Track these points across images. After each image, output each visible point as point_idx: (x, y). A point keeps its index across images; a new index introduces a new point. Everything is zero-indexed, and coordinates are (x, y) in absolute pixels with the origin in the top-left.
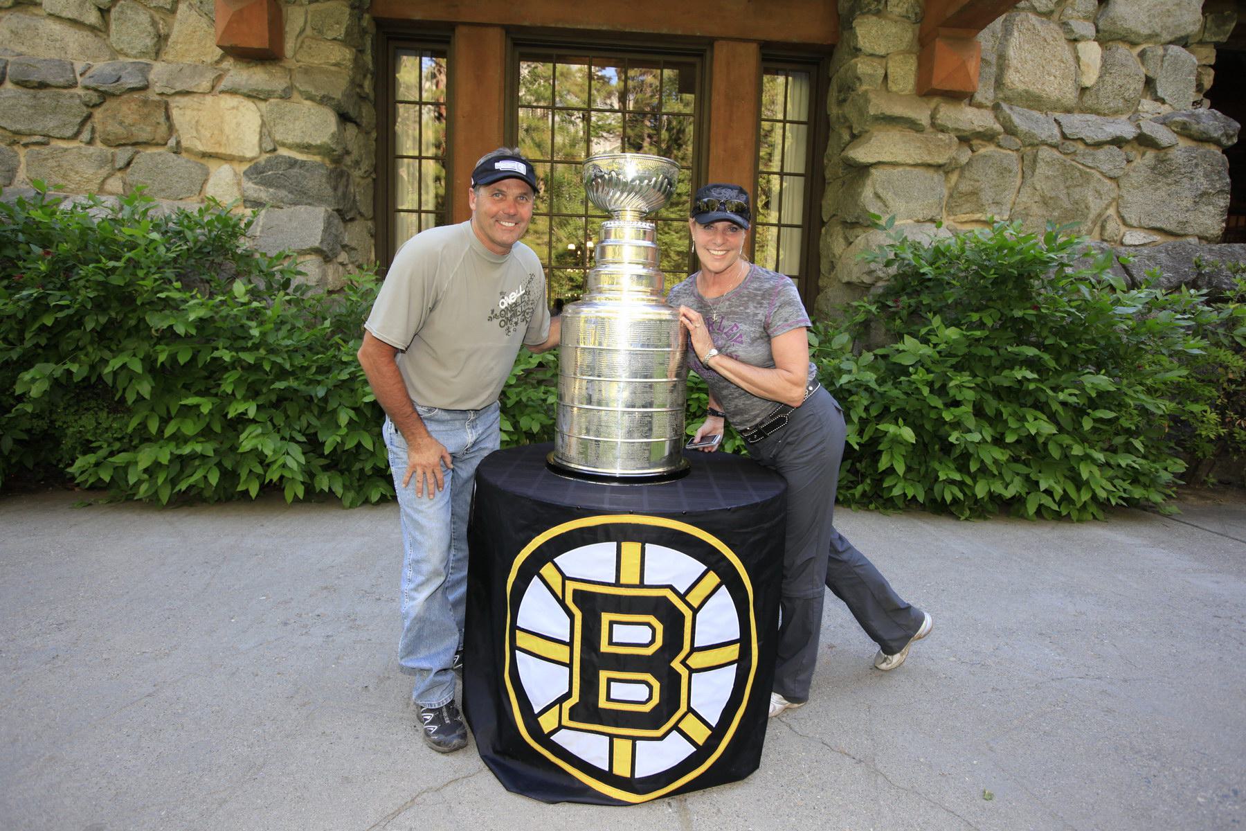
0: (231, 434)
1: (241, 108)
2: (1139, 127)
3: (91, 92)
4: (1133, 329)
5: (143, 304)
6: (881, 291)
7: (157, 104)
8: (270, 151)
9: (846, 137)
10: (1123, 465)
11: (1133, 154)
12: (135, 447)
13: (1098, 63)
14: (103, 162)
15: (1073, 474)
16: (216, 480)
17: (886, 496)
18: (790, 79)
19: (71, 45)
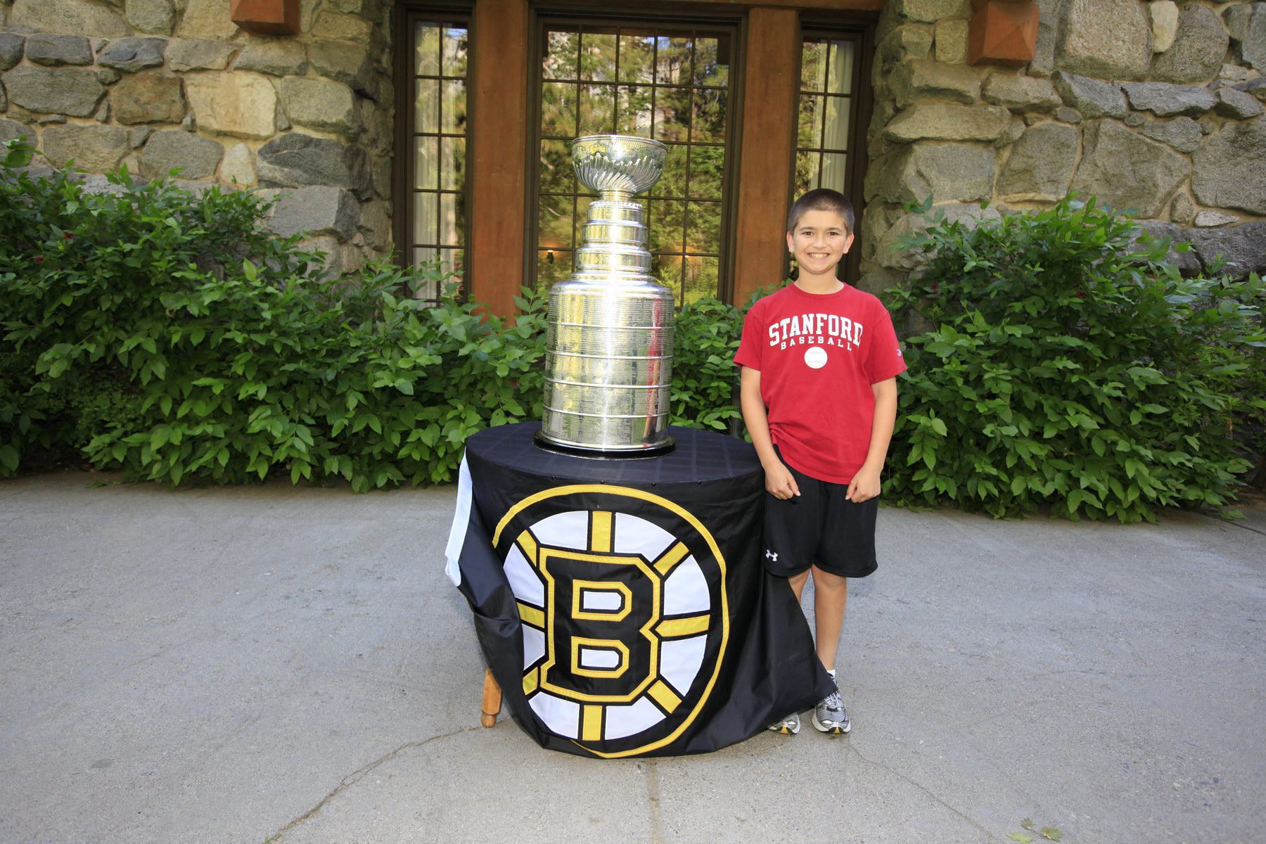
0: (242, 416)
1: (256, 85)
2: (1218, 95)
3: (107, 69)
4: (1189, 319)
5: (157, 285)
6: (920, 276)
7: (172, 82)
8: (286, 130)
9: (889, 111)
10: (1175, 464)
11: (1210, 126)
12: (149, 429)
13: (1175, 25)
14: (119, 141)
15: (1119, 473)
16: (227, 461)
17: (916, 491)
18: (834, 48)
19: (88, 21)
